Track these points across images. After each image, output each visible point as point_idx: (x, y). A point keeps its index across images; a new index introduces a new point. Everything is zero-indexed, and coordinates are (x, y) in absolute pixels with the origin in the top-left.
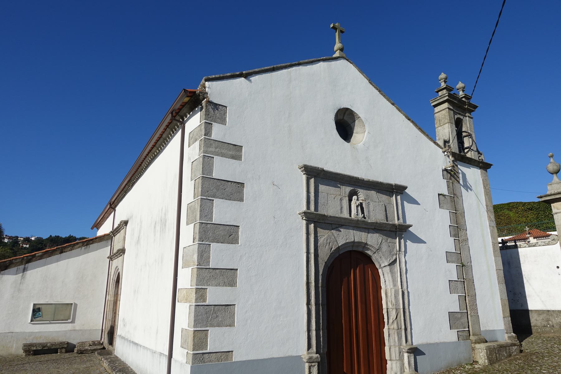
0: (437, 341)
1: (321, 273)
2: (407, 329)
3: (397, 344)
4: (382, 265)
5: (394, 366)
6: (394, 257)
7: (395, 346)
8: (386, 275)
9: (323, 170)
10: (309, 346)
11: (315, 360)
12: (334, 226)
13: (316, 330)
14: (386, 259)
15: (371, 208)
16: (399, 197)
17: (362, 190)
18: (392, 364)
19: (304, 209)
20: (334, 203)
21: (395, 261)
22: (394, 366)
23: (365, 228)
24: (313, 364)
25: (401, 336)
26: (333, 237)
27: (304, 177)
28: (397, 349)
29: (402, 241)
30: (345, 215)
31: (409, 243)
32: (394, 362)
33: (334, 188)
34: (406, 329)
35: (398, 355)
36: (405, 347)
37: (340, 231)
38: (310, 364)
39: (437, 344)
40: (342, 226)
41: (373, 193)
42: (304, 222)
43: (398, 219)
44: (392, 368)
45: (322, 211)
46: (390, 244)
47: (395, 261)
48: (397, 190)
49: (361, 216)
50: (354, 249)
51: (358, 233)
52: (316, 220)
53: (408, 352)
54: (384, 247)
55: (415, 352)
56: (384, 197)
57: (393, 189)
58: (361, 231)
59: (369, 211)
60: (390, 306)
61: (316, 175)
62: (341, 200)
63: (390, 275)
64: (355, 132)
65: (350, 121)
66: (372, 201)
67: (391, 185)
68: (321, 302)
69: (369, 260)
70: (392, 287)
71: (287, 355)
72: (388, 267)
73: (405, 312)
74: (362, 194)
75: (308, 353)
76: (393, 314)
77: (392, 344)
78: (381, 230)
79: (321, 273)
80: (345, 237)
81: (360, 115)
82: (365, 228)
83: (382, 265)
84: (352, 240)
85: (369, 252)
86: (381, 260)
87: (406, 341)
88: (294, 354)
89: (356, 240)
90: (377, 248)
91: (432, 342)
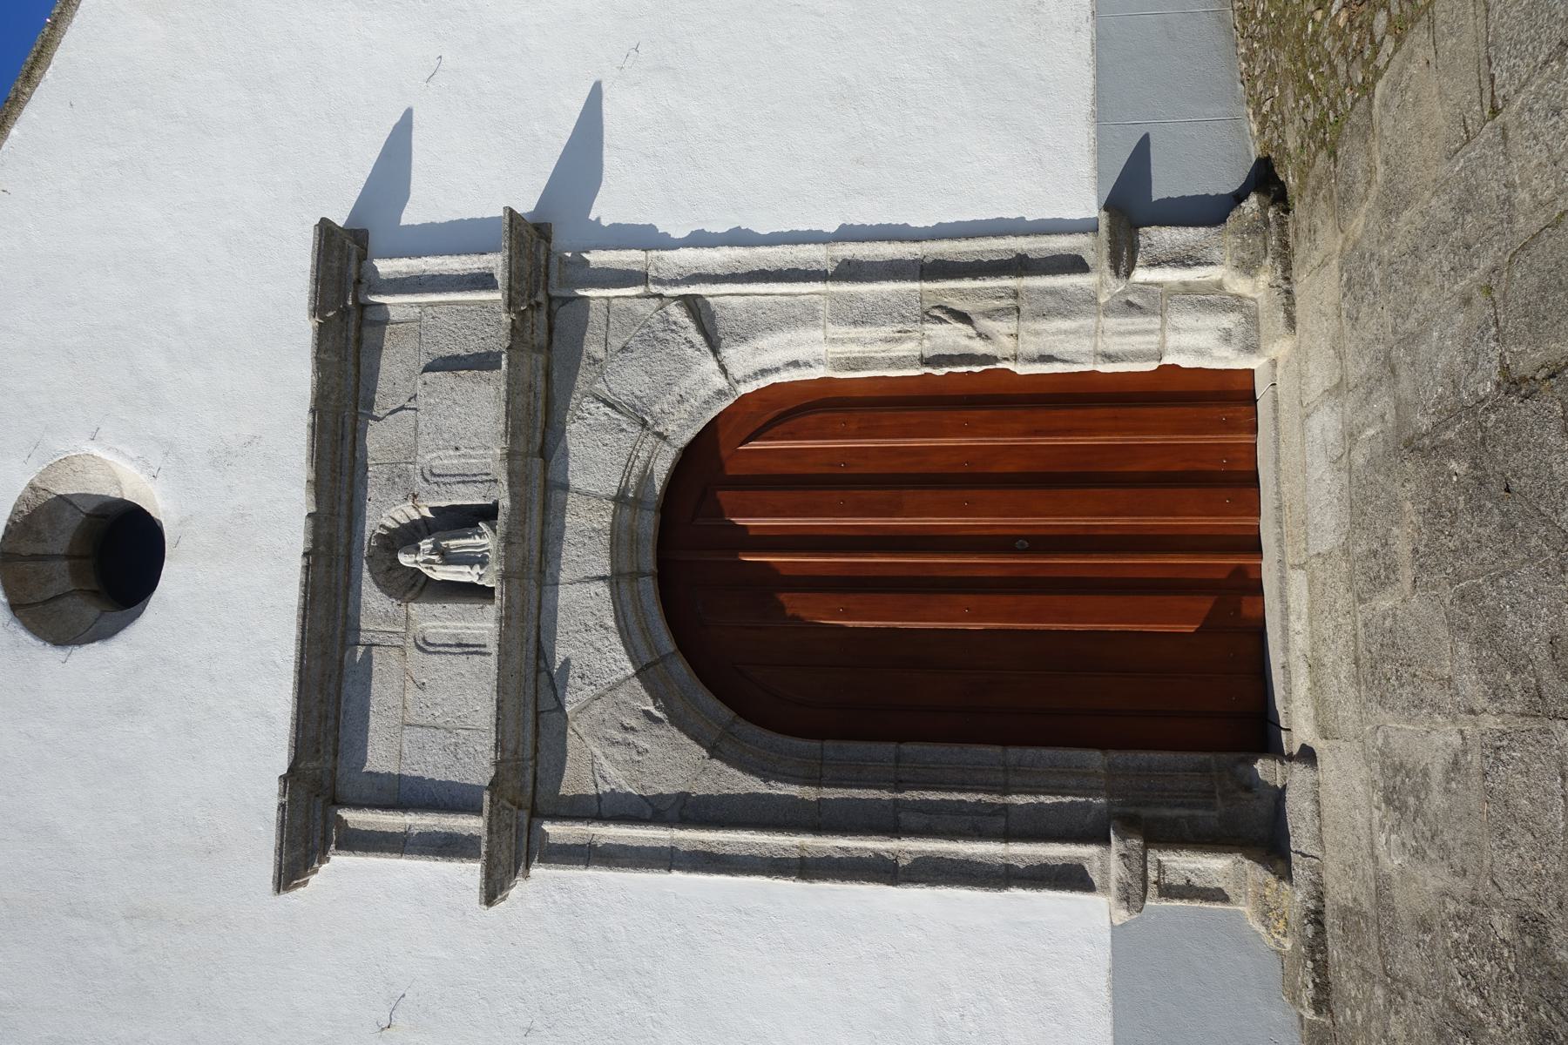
0: (1086, 38)
1: (752, 785)
2: (1015, 261)
3: (1089, 322)
4: (720, 382)
5: (1187, 340)
6: (677, 313)
7: (1097, 332)
8: (766, 360)
9: (291, 779)
10: (1073, 878)
11: (1136, 867)
12: (547, 702)
13: (1007, 836)
14: (686, 367)
15: (447, 461)
16: (386, 267)
17: (371, 509)
18: (1180, 351)
19: (470, 873)
20: (434, 700)
21: (693, 305)
22: (1187, 340)
23: (545, 507)
24: (1152, 875)
25: (1052, 292)
26: (597, 707)
27: (339, 862)
28: (1111, 323)
29: (597, 258)
30: (483, 624)
31: (607, 209)
32: (1173, 340)
33: (375, 685)
34: (1021, 265)
35: (1139, 322)
36: (1098, 281)
37: (567, 662)
38: (1153, 890)
39: (1101, 43)
40: (541, 653)
41: (378, 440)
42: (538, 871)
43: (483, 281)
44: (1200, 352)
45: (475, 765)
46: (616, 343)
47: (693, 305)
48: (345, 269)
49: (485, 540)
50: (648, 561)
51: (569, 553)
52: (521, 816)
53: (1128, 275)
54: (629, 380)
55: (1131, 210)
56: (396, 368)
57: (344, 313)
58: (560, 538)
59: (466, 479)
60: (908, 348)
61: (325, 802)
62: (425, 646)
63: (764, 342)
64: (114, 493)
65: (71, 522)
66: (413, 450)
67: (322, 333)
68: (886, 795)
69: (702, 457)
70: (819, 334)
71: (1105, 996)
72: (730, 354)
73: (938, 264)
74: (386, 511)
75: (1105, 889)
76: (950, 337)
77: (1087, 344)
78: (548, 413)
79: (752, 785)
80: (593, 642)
81: (21, 486)
82: (545, 507)
83: (720, 382)
84: (603, 589)
85: (662, 468)
86: (691, 392)
87: (1075, 264)
88: (1103, 956)
89: (603, 566)
90: (636, 430)
91: (1089, 82)
